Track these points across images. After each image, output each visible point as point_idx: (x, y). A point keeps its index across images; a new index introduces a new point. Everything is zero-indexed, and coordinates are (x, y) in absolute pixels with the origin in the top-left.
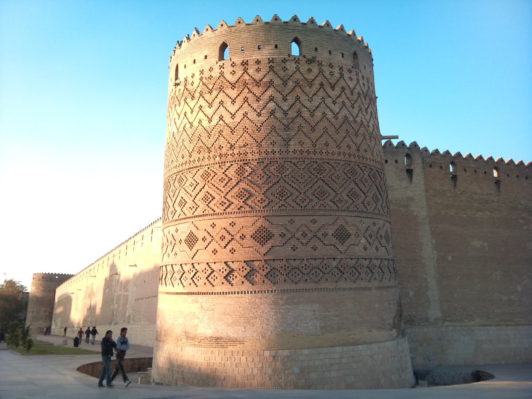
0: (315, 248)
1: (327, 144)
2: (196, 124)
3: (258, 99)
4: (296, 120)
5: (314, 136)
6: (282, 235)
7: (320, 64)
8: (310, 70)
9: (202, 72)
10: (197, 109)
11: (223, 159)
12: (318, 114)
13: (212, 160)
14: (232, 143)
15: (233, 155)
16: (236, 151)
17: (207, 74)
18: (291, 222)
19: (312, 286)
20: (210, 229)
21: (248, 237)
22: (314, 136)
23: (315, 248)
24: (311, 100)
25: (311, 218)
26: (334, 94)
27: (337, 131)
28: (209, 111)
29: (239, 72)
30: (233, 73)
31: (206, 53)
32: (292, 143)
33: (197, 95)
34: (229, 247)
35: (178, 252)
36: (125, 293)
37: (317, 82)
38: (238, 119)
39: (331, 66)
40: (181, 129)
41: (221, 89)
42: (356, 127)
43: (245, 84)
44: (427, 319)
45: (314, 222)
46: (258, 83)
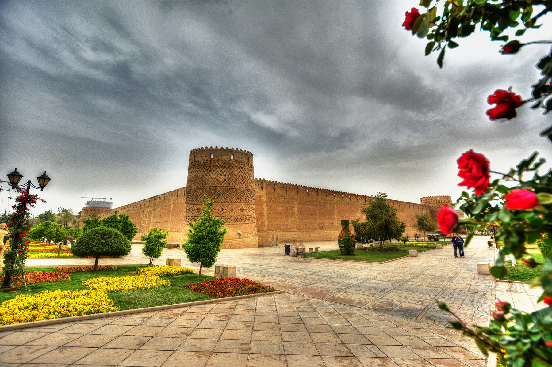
0: (235, 213)
1: (239, 185)
2: (201, 176)
7: (239, 162)
9: (204, 160)
10: (202, 171)
11: (210, 187)
15: (213, 186)
16: (214, 185)
17: (206, 161)
19: (233, 223)
21: (217, 210)
22: (236, 182)
23: (235, 213)
24: (236, 172)
26: (242, 170)
27: (243, 181)
28: (206, 172)
31: (206, 155)
33: (202, 167)
35: (194, 213)
37: (238, 167)
38: (215, 176)
39: (242, 162)
41: (210, 167)
42: (247, 179)
44: (264, 230)
45: (235, 206)
46: (221, 166)
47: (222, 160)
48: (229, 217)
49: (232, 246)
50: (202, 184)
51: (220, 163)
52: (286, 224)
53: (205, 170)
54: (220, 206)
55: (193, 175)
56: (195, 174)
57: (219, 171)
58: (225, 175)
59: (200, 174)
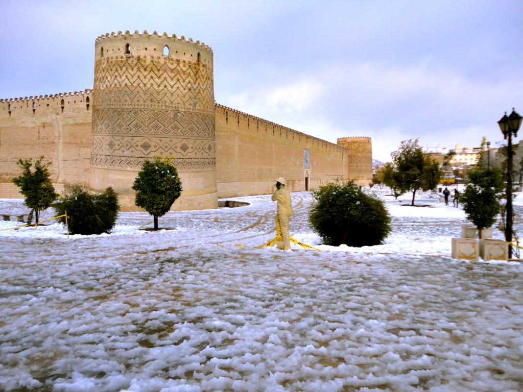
2: (148, 85)
3: (184, 81)
4: (199, 95)
5: (204, 103)
6: (192, 148)
7: (206, 68)
8: (203, 70)
9: (152, 57)
10: (149, 77)
12: (205, 92)
13: (160, 108)
14: (172, 101)
16: (174, 106)
18: (195, 142)
23: (202, 154)
28: (158, 81)
29: (175, 65)
30: (172, 64)
31: (155, 47)
32: (197, 105)
33: (149, 69)
34: (169, 151)
37: (205, 77)
40: (135, 84)
41: (165, 71)
43: (178, 72)
45: (202, 142)
46: (184, 72)
47: (184, 62)
48: (196, 160)
49: (202, 205)
50: (152, 101)
51: (181, 65)
52: (226, 171)
53: (154, 76)
54: (183, 142)
55: (126, 81)
56: (132, 80)
57: (181, 81)
58: (190, 89)
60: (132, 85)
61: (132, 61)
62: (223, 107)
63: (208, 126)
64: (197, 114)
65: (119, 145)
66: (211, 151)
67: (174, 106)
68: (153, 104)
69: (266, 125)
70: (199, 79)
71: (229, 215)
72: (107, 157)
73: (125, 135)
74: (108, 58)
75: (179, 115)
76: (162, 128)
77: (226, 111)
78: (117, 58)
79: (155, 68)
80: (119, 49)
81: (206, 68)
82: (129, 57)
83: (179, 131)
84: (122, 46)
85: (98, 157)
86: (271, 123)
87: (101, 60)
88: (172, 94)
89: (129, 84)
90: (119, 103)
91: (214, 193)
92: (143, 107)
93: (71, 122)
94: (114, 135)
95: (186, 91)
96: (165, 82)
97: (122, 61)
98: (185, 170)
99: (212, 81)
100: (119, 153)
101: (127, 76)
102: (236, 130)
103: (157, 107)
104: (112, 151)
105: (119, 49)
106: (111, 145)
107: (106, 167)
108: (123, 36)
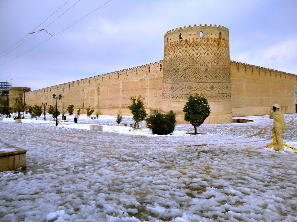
2: (191, 55)
3: (211, 50)
5: (224, 61)
6: (216, 88)
7: (225, 40)
8: (223, 42)
9: (193, 39)
10: (191, 50)
12: (224, 55)
13: (198, 66)
14: (204, 62)
15: (204, 65)
16: (205, 64)
20: (197, 85)
23: (222, 91)
25: (222, 83)
28: (197, 51)
29: (206, 41)
30: (205, 41)
31: (195, 33)
32: (219, 63)
33: (191, 46)
36: (91, 97)
41: (201, 45)
43: (208, 45)
45: (222, 84)
46: (211, 45)
47: (211, 39)
48: (218, 95)
49: (222, 121)
50: (193, 63)
51: (210, 41)
52: (237, 100)
54: (211, 84)
55: (180, 54)
56: (183, 53)
57: (210, 50)
58: (215, 54)
59: (189, 53)
60: (183, 55)
61: (183, 43)
62: (235, 62)
63: (226, 74)
64: (219, 68)
65: (176, 88)
66: (228, 89)
67: (205, 64)
68: (194, 64)
69: (265, 71)
70: (220, 48)
71: (240, 128)
72: (170, 95)
73: (179, 82)
74: (171, 43)
75: (209, 69)
76: (199, 78)
77: (237, 64)
78: (175, 42)
79: (195, 45)
80: (176, 38)
81: (225, 40)
82: (181, 41)
83: (209, 78)
84: (178, 36)
85: (165, 95)
86: (269, 70)
87: (167, 45)
88: (204, 58)
89: (181, 55)
90: (176, 66)
91: (230, 114)
92: (188, 67)
93: (153, 78)
94: (173, 83)
95: (212, 55)
96: (201, 51)
97: (177, 44)
98: (212, 101)
99: (229, 47)
100: (176, 92)
101: (180, 51)
102: (244, 76)
103: (196, 66)
104: (172, 91)
105: (176, 38)
106: (172, 88)
107: (170, 100)
108: (178, 30)
